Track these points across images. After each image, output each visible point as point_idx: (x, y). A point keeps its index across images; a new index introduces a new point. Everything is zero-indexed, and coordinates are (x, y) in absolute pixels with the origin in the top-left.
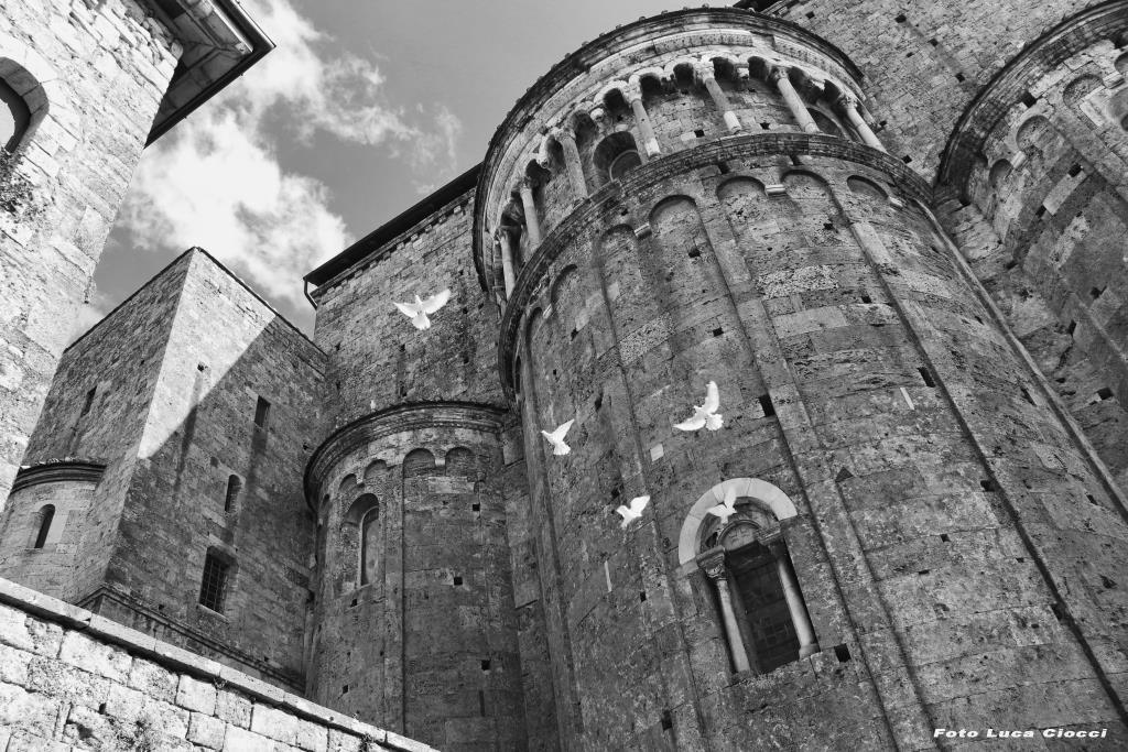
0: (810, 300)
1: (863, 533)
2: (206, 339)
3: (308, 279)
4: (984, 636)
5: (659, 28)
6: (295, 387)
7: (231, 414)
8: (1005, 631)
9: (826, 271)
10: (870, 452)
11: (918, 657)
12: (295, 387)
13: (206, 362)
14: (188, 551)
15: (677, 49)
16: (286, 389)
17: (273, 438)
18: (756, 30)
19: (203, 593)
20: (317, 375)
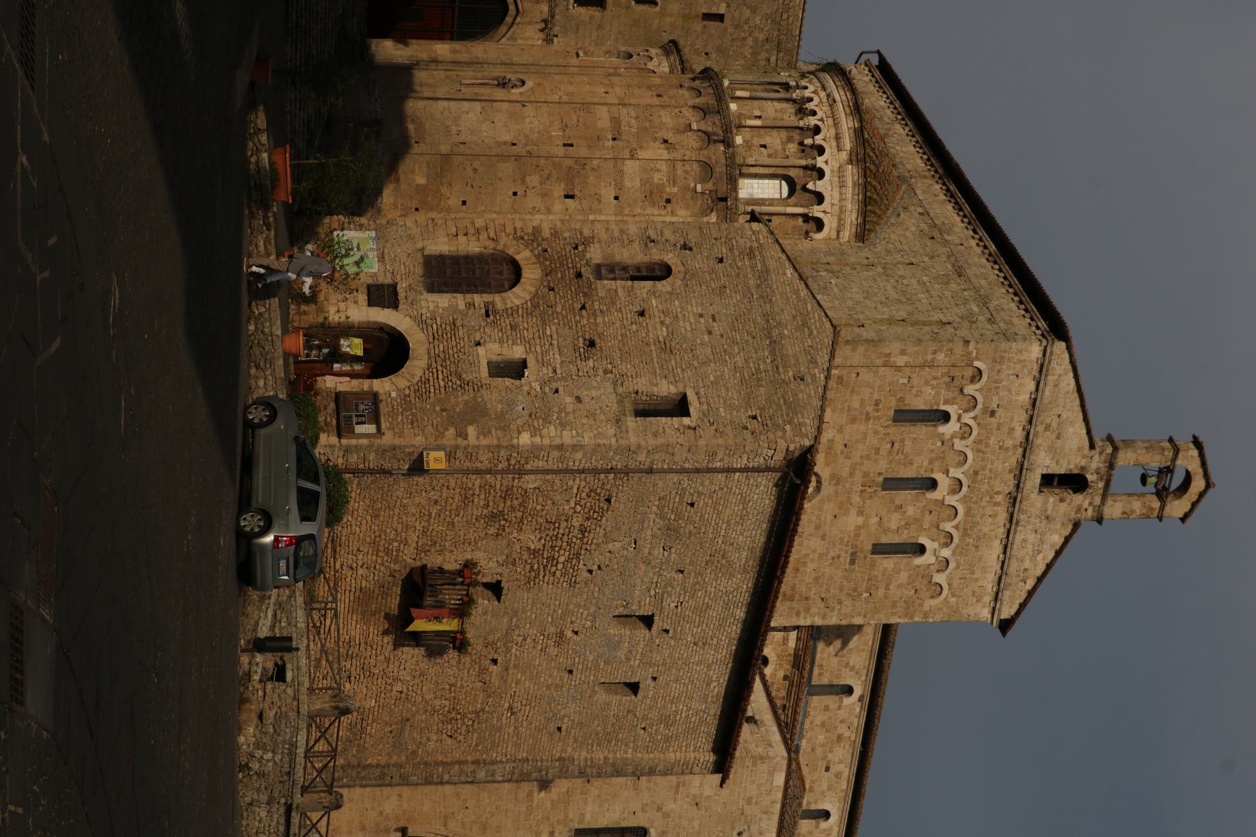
0: (616, 121)
1: (499, 103)
3: (878, 52)
4: (457, 120)
5: (851, 104)
6: (750, 41)
8: (456, 125)
9: (633, 130)
10: (532, 114)
11: (452, 103)
12: (750, 41)
15: (832, 113)
16: (743, 35)
17: (699, 28)
18: (854, 154)
20: (773, 59)
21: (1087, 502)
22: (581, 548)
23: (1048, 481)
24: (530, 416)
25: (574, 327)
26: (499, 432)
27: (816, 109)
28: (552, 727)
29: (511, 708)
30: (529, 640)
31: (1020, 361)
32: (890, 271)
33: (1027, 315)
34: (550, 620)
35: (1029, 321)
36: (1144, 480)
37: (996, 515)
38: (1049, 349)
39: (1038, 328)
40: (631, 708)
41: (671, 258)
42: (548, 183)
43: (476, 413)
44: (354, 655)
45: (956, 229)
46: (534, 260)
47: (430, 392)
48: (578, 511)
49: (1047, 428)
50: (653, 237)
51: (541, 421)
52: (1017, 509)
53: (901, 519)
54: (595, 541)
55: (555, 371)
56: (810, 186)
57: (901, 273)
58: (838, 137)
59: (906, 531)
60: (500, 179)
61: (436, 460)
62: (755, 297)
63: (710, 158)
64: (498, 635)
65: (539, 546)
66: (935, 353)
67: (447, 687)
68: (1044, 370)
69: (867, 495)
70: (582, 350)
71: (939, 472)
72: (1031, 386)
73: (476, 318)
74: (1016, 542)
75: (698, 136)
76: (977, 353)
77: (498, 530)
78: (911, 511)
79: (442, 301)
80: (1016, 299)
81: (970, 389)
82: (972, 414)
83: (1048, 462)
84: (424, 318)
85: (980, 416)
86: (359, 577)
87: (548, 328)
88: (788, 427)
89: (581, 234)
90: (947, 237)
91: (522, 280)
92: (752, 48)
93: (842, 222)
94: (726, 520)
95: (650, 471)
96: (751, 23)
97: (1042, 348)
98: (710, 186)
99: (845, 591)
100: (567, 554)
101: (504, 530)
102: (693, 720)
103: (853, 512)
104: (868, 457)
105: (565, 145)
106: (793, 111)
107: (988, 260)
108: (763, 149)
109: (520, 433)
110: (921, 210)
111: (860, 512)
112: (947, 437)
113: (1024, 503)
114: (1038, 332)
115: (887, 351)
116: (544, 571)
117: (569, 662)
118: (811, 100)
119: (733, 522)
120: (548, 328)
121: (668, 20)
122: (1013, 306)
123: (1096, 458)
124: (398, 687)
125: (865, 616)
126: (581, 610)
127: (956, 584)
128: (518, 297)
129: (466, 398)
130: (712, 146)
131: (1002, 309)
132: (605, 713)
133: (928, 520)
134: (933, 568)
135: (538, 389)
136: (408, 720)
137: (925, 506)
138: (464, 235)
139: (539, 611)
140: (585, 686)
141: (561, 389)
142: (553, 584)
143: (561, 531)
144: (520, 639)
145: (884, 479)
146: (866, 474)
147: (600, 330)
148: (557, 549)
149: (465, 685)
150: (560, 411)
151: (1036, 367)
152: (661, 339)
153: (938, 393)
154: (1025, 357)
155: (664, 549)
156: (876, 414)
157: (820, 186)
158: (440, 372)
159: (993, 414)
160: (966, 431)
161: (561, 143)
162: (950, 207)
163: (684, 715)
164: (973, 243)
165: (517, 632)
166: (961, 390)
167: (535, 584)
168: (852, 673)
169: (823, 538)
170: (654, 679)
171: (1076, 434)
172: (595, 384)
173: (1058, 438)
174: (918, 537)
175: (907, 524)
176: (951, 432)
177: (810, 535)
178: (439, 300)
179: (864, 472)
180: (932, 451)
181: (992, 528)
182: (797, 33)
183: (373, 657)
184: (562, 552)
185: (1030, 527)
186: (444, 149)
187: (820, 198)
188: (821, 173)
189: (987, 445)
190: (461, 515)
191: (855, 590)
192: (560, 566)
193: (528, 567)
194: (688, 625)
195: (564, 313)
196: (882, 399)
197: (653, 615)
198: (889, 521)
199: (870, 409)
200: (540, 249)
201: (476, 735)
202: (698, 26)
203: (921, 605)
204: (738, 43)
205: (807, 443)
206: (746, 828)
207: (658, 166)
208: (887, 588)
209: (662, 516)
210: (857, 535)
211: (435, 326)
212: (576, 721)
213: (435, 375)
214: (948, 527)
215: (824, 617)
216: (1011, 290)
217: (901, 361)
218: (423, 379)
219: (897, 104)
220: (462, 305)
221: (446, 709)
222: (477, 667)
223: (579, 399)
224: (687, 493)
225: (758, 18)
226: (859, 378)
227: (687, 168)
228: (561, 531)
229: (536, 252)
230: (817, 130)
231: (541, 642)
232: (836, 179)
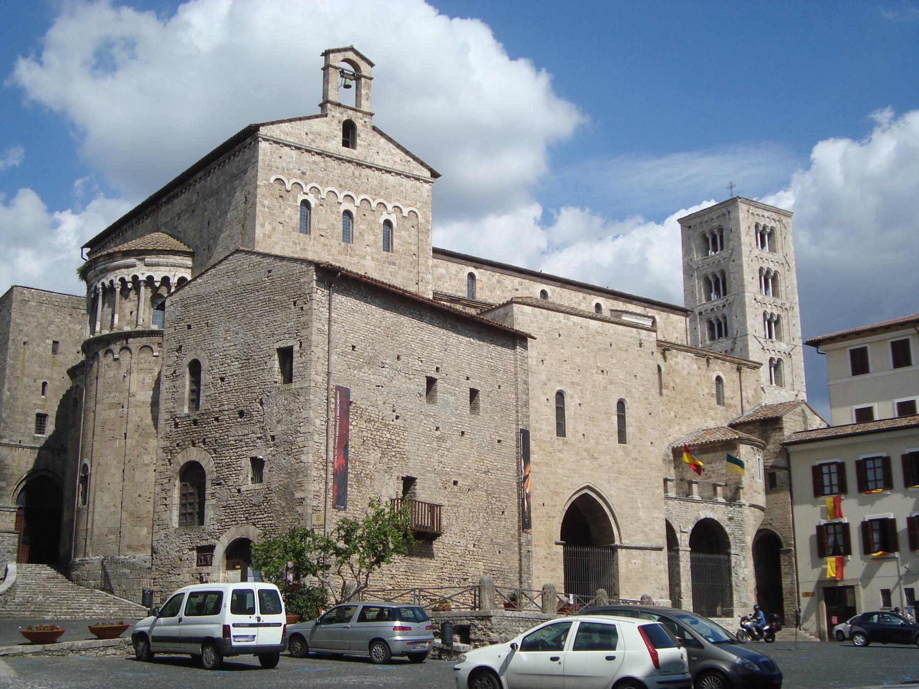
2: (26, 329)
3: (82, 248)
4: (106, 508)
7: (40, 357)
13: (26, 339)
14: (28, 418)
16: (67, 330)
17: (62, 357)
18: (138, 257)
19: (37, 429)
21: (360, 121)
22: (381, 422)
23: (346, 144)
24: (289, 454)
25: (230, 425)
26: (300, 476)
27: (109, 280)
28: (497, 445)
29: (485, 473)
30: (442, 460)
31: (271, 155)
32: (213, 235)
33: (243, 150)
34: (429, 445)
35: (246, 149)
36: (347, 87)
37: (367, 175)
38: (265, 137)
39: (250, 144)
40: (486, 394)
41: (187, 361)
42: (149, 449)
43: (287, 492)
44: (450, 576)
45: (189, 197)
46: (185, 451)
47: (271, 524)
48: (356, 424)
49: (314, 141)
50: (173, 372)
51: (293, 447)
52: (363, 163)
53: (368, 233)
54: (377, 413)
55: (260, 438)
56: (157, 284)
57: (214, 229)
58: (127, 267)
59: (376, 230)
60: (145, 480)
61: (318, 520)
62: (214, 303)
63: (137, 347)
64: (438, 480)
65: (379, 451)
66: (264, 206)
67: (471, 514)
68: (277, 140)
69: (353, 253)
70: (245, 420)
71: (339, 208)
72: (287, 149)
73: (223, 493)
74: (384, 165)
75: (123, 354)
77: (367, 478)
78: (363, 227)
79: (209, 513)
80: (232, 158)
81: (289, 187)
82: (304, 186)
83: (334, 142)
84: (220, 527)
85: (305, 181)
86: (398, 573)
87: (230, 443)
88: (302, 280)
89: (169, 420)
90: (194, 202)
91: (197, 460)
92: (75, 325)
93: (181, 265)
94: (364, 325)
95: (328, 374)
96: (59, 324)
97: (263, 141)
98: (155, 347)
99: (412, 269)
100: (385, 432)
101: (368, 474)
102: (494, 355)
103: (363, 262)
104: (329, 251)
105: (126, 439)
106: (110, 294)
107: (208, 176)
108: (133, 314)
109: (301, 462)
110: (177, 218)
111: (364, 258)
112: (317, 202)
113: (360, 158)
114: (253, 143)
115: (262, 235)
116: (395, 448)
117: (456, 433)
118: (103, 284)
119: (366, 320)
120: (230, 443)
121: (55, 376)
122: (237, 159)
123: (333, 113)
124: (471, 547)
125: (428, 258)
126: (423, 424)
128: (209, 462)
129: (276, 498)
130: (129, 346)
131: (238, 166)
132: (489, 411)
133: (370, 217)
134: (399, 215)
135: (272, 449)
136: (492, 540)
137: (361, 218)
138: (166, 500)
139: (423, 453)
140: (472, 423)
141: (272, 434)
142: (405, 442)
143: (369, 435)
144: (440, 465)
145: (343, 241)
146: (340, 253)
147: (233, 407)
148: (381, 439)
149: (470, 502)
150: (286, 433)
151: (275, 145)
152: (241, 366)
153: (289, 206)
154: (269, 151)
155: (383, 367)
156: (302, 244)
157: (158, 278)
158: (258, 517)
159: (304, 173)
160: (317, 191)
161: (123, 441)
162: (176, 201)
163: (491, 360)
164: (198, 186)
165: (436, 467)
166: (288, 191)
167: (405, 455)
168: (461, 272)
170: (468, 379)
171: (317, 125)
172: (269, 410)
173: (320, 135)
174: (379, 223)
175: (371, 229)
178: (209, 517)
179: (339, 254)
180: (326, 211)
181: (375, 178)
182: (67, 296)
183: (451, 563)
184: (384, 436)
185: (375, 156)
186: (125, 515)
187: (165, 281)
188: (150, 278)
189: (323, 178)
190: (357, 503)
191: (411, 263)
192: (393, 437)
193: (393, 459)
194: (434, 354)
195: (220, 431)
196: (292, 240)
197: (426, 377)
198: (369, 240)
200: (177, 448)
201: (502, 496)
202: (60, 357)
203: (421, 225)
204: (72, 332)
205: (312, 268)
207: (141, 380)
208: (411, 244)
209: (361, 367)
210: (378, 260)
211: (226, 520)
212: (494, 430)
213: (260, 520)
214: (374, 205)
215: (428, 283)
216: (227, 161)
217: (268, 227)
218: (262, 528)
219: (113, 236)
220: (214, 502)
221: (485, 515)
222: (458, 494)
223: (278, 422)
224: (346, 349)
225: (56, 320)
227: (143, 361)
228: (369, 435)
229: (179, 450)
230: (122, 280)
231: (443, 452)
232: (154, 268)
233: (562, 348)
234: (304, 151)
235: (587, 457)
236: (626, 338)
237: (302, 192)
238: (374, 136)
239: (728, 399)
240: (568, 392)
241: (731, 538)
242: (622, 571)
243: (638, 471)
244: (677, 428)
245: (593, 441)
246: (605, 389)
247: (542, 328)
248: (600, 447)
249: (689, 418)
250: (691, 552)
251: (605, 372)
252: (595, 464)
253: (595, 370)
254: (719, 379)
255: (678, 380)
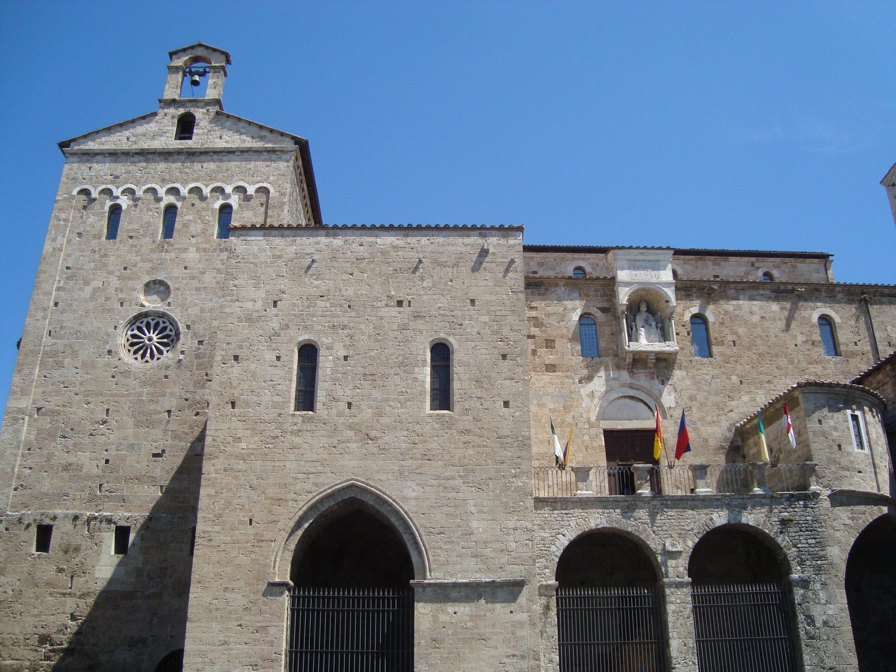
49: (135, 143)
53: (195, 222)
66: (59, 220)
76: (65, 194)
81: (95, 194)
103: (184, 255)
111: (186, 250)
112: (131, 203)
115: (51, 250)
127: (256, 179)
134: (242, 196)
137: (187, 209)
146: (152, 251)
156: (103, 251)
159: (117, 177)
169: (203, 273)
173: (145, 136)
176: (127, 201)
177: (199, 283)
179: (151, 252)
196: (91, 248)
199: (97, 256)
206: (308, 256)
226: (70, 266)
233: (317, 279)
234: (120, 155)
235: (354, 438)
236: (455, 248)
237: (112, 198)
238: (217, 121)
239: (847, 345)
240: (323, 341)
241: (792, 553)
242: (422, 627)
243: (470, 451)
244: (745, 398)
245: (370, 411)
246: (403, 328)
247: (280, 257)
248: (384, 420)
249: (769, 382)
250: (693, 584)
251: (405, 304)
252: (372, 447)
253: (384, 303)
254: (825, 320)
255: (741, 331)
